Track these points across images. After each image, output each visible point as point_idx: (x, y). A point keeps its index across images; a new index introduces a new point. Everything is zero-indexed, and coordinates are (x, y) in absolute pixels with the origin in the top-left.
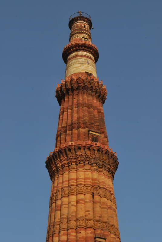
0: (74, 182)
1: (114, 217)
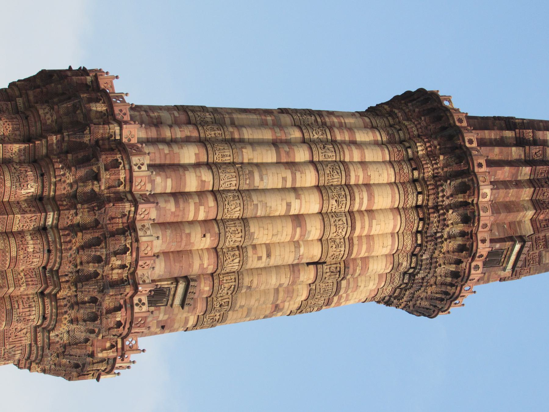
0: (361, 204)
1: (248, 319)
